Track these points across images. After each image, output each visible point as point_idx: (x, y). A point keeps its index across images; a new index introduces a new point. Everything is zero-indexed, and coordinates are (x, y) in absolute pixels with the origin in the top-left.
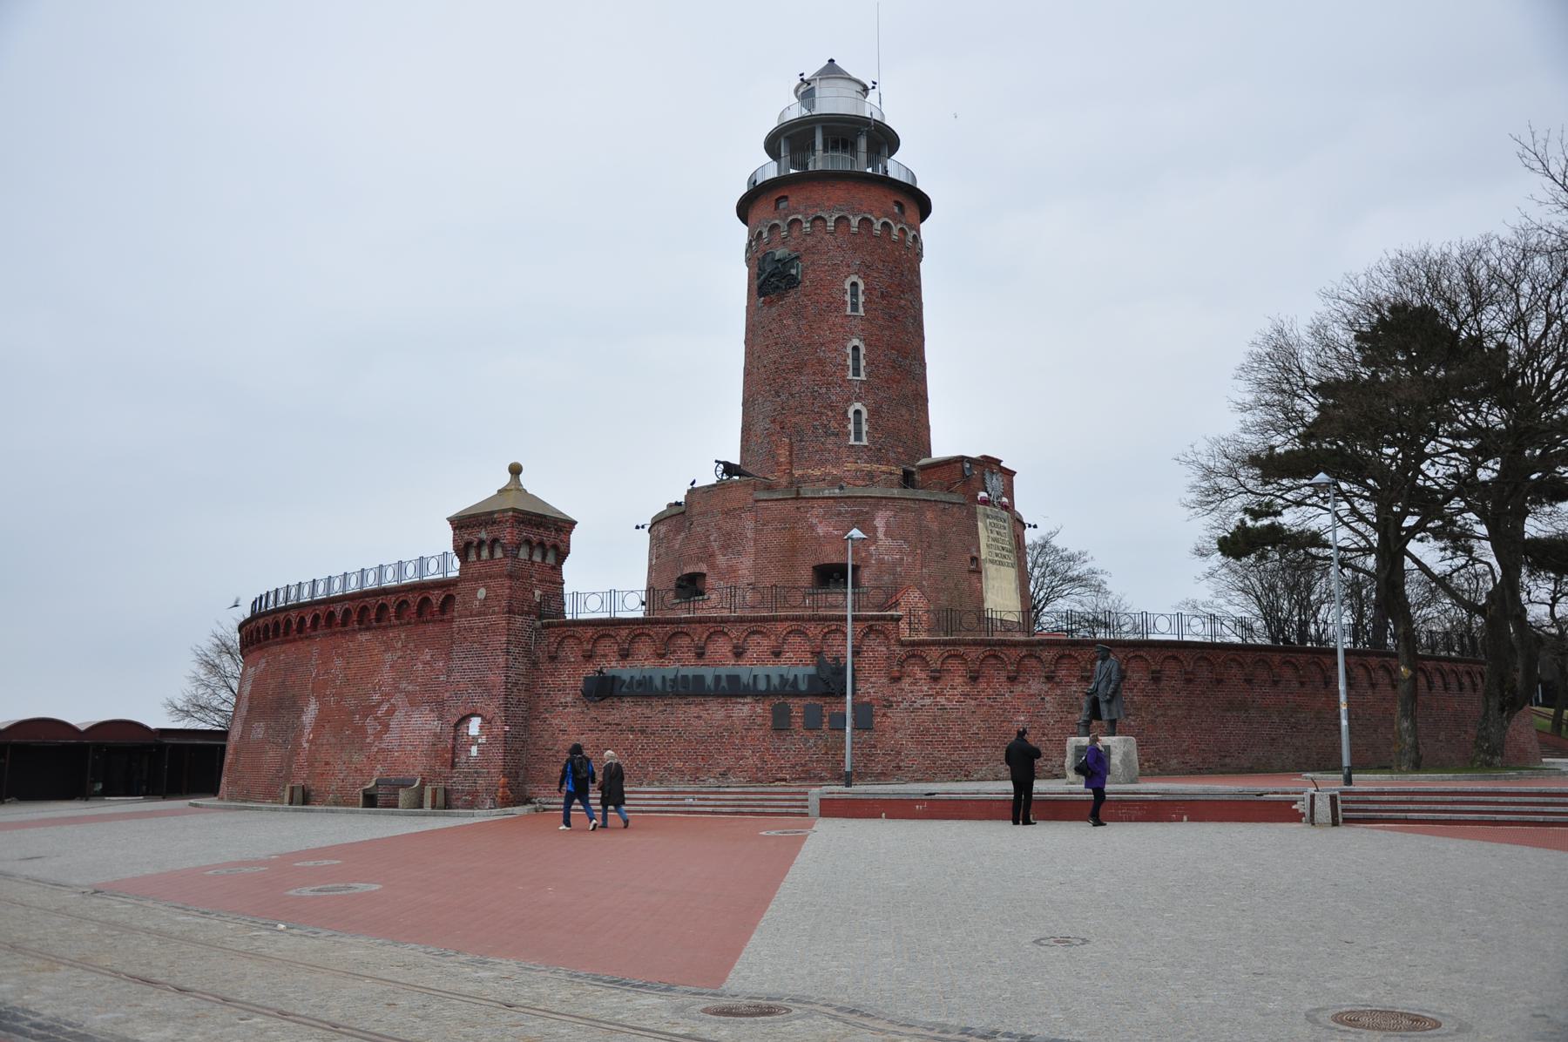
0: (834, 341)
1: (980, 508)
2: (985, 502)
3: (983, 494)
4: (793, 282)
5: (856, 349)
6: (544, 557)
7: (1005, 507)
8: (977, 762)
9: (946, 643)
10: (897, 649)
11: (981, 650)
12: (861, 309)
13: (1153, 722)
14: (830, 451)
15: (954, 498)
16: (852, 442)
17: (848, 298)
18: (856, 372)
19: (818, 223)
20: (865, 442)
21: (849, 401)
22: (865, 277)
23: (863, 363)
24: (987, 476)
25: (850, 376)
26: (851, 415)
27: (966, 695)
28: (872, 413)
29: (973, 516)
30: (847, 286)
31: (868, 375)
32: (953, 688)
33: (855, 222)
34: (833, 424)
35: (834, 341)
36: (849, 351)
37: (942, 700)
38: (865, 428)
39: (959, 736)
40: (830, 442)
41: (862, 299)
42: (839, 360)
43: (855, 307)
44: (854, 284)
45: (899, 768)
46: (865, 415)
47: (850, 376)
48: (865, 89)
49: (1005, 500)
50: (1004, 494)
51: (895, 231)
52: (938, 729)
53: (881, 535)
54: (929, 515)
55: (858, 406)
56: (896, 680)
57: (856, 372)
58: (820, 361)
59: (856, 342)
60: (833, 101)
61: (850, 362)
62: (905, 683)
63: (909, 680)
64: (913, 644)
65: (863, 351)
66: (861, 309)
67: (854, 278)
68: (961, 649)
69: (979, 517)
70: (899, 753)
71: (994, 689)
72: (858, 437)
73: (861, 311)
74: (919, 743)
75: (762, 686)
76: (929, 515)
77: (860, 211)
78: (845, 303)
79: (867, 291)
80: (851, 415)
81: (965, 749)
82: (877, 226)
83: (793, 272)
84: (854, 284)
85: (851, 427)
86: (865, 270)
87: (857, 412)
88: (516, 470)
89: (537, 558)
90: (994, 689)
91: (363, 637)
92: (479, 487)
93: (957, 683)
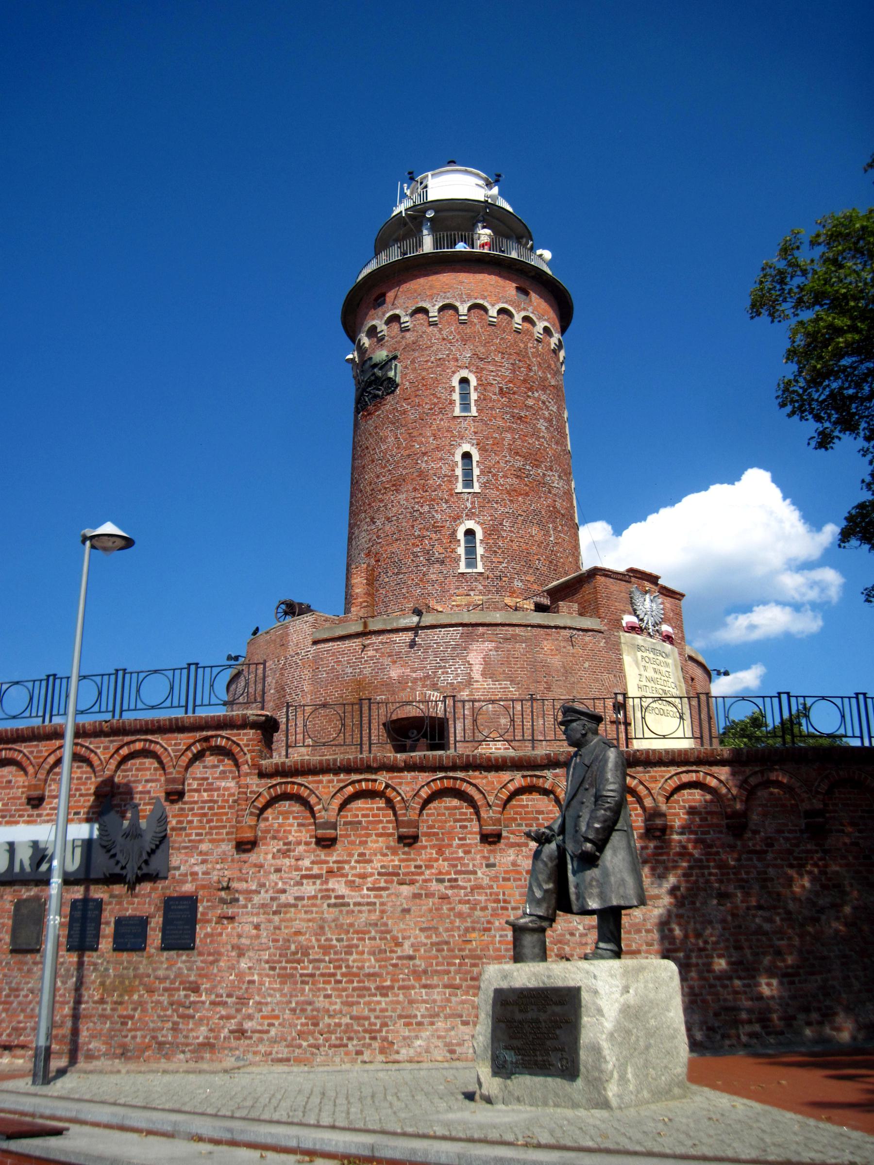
0: (438, 448)
1: (625, 637)
2: (632, 629)
3: (628, 619)
4: (391, 385)
5: (467, 456)
7: (668, 638)
8: (408, 1019)
9: (348, 769)
10: (254, 783)
11: (424, 777)
12: (474, 409)
14: (433, 583)
15: (587, 623)
16: (463, 569)
17: (456, 396)
18: (468, 483)
19: (420, 316)
20: (480, 568)
21: (457, 518)
22: (478, 371)
23: (476, 472)
24: (637, 596)
25: (459, 488)
26: (460, 535)
27: (390, 874)
28: (487, 534)
29: (616, 647)
30: (455, 382)
31: (484, 486)
32: (363, 859)
34: (438, 549)
35: (438, 448)
36: (458, 458)
37: (338, 886)
38: (480, 550)
39: (371, 964)
40: (434, 572)
41: (474, 396)
42: (445, 470)
43: (466, 406)
44: (464, 381)
45: (240, 1033)
46: (479, 535)
47: (459, 488)
49: (666, 628)
50: (664, 620)
51: (518, 318)
52: (326, 949)
53: (477, 675)
54: (547, 646)
55: (470, 524)
56: (245, 846)
57: (468, 483)
58: (422, 474)
59: (466, 447)
61: (459, 472)
62: (265, 854)
63: (275, 846)
64: (281, 772)
65: (476, 457)
66: (474, 409)
67: (464, 373)
68: (382, 779)
69: (624, 647)
70: (242, 1001)
71: (454, 862)
72: (471, 561)
73: (474, 412)
74: (285, 977)
76: (547, 645)
77: (469, 296)
78: (452, 402)
79: (482, 385)
80: (460, 535)
81: (384, 991)
82: (493, 312)
83: (391, 374)
84: (464, 381)
85: (461, 550)
86: (478, 362)
87: (470, 533)
90: (454, 862)
93: (371, 848)
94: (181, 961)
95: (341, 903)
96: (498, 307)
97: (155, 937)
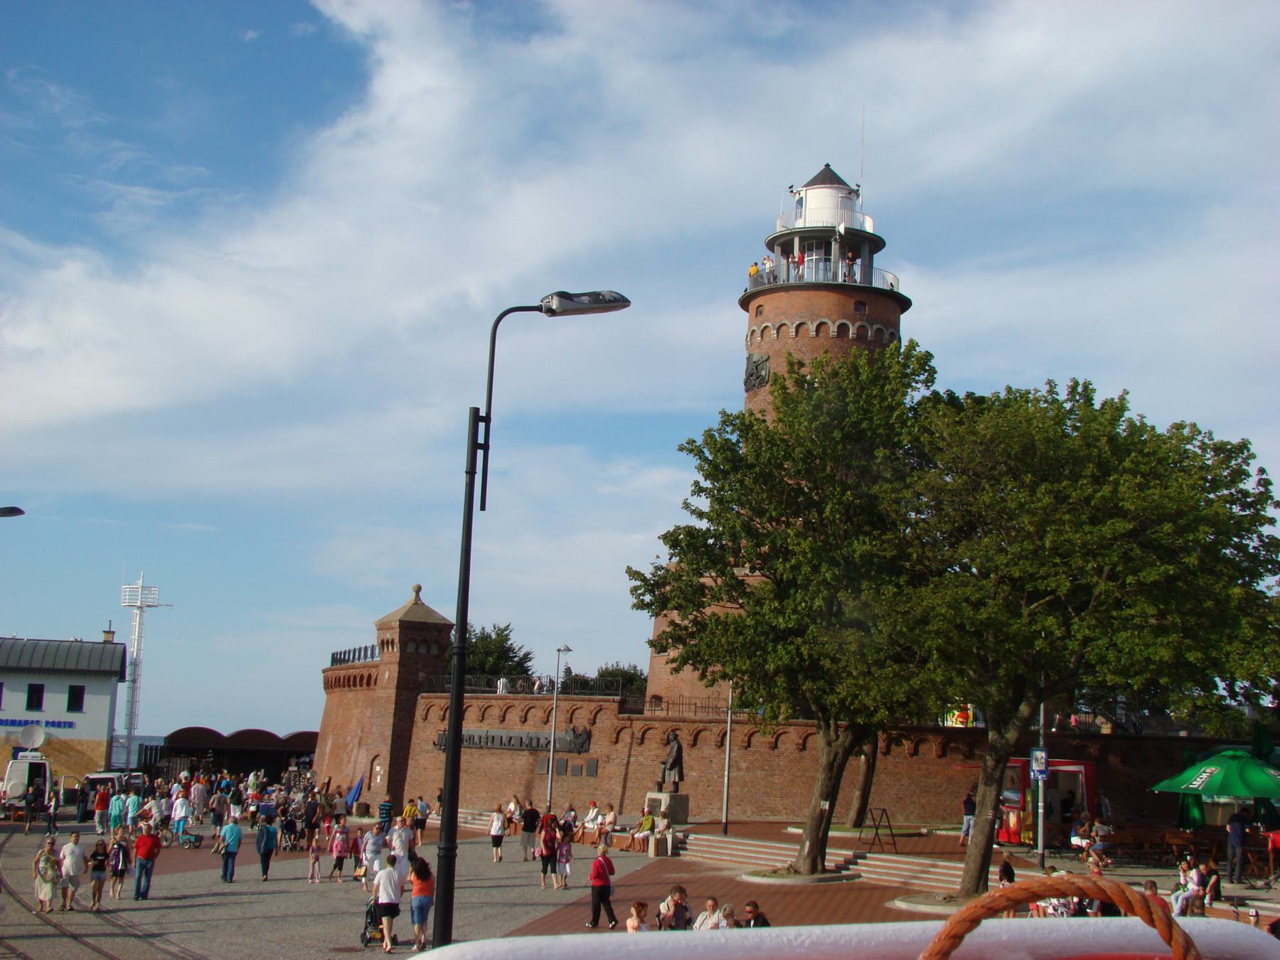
6: (428, 650)
11: (670, 724)
13: (792, 781)
33: (812, 327)
48: (851, 192)
60: (820, 209)
75: (534, 744)
77: (818, 316)
88: (418, 589)
89: (423, 650)
91: (351, 695)
92: (397, 603)
94: (592, 780)
95: (641, 765)
96: (837, 323)
97: (584, 772)
